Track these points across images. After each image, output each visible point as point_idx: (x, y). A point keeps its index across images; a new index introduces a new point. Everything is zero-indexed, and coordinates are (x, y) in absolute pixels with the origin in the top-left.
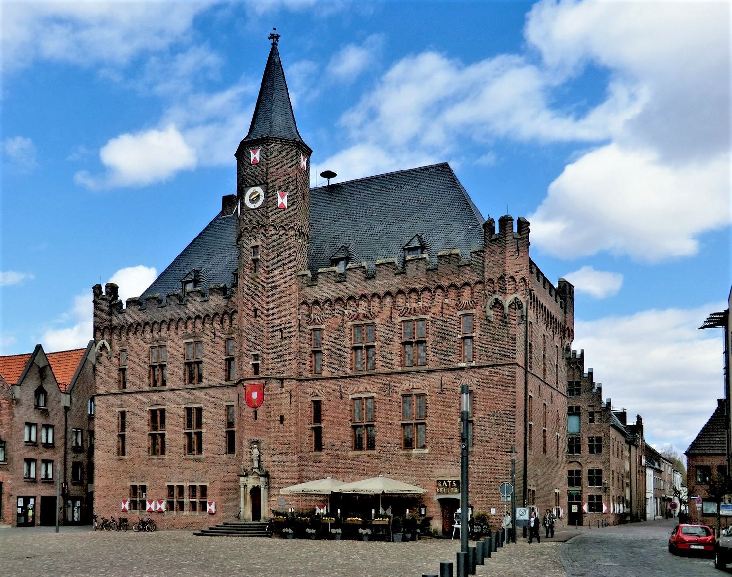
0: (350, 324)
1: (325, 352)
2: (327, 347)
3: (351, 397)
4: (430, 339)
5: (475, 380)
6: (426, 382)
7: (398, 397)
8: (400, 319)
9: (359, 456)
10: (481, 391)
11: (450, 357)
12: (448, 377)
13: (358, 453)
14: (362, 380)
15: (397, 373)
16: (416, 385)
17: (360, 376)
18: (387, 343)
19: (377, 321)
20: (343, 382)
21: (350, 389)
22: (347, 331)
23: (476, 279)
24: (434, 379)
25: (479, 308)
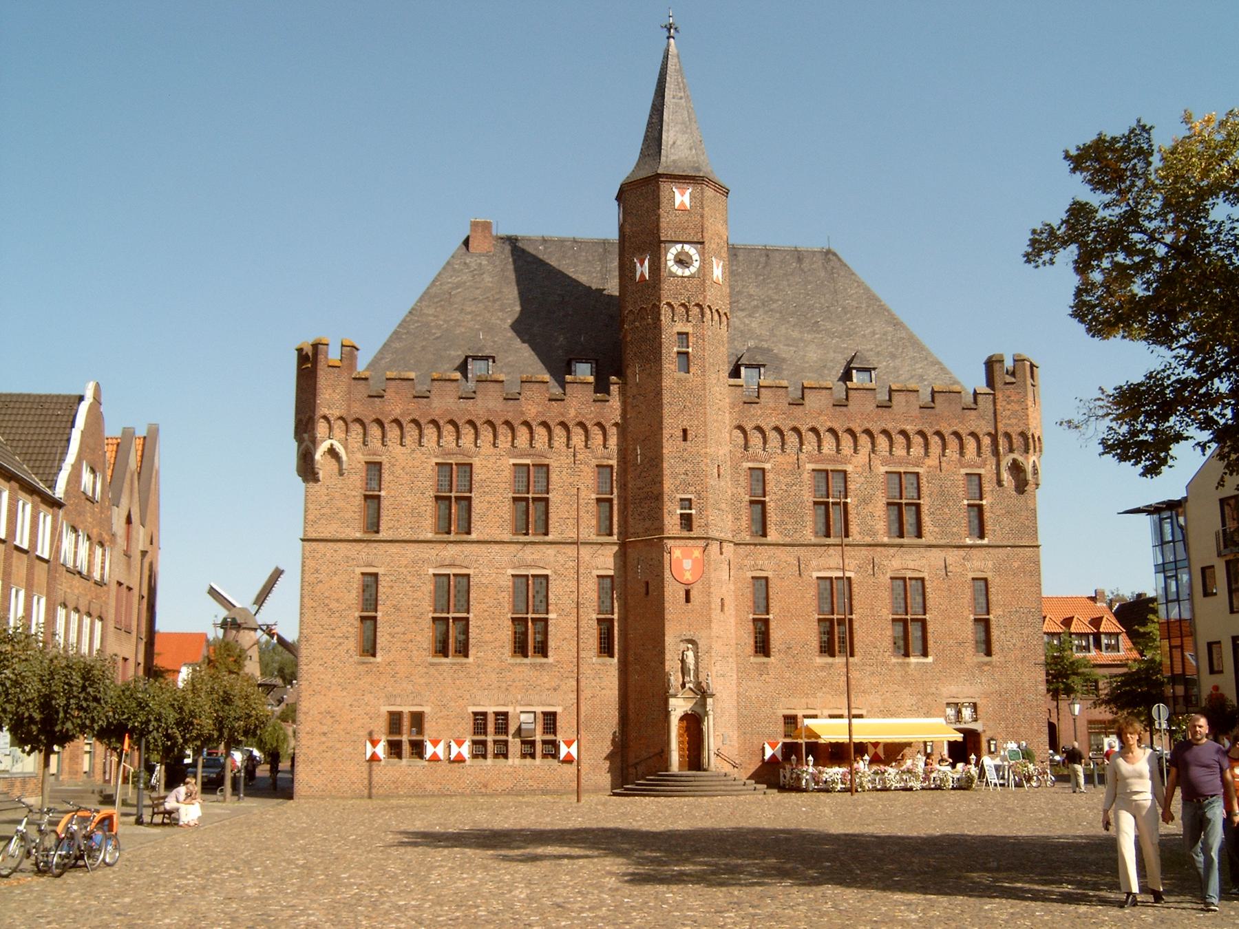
0: (810, 466)
1: (772, 504)
2: (774, 497)
3: (815, 574)
4: (925, 502)
5: (990, 564)
6: (924, 561)
7: (885, 579)
8: (883, 469)
9: (831, 665)
10: (998, 579)
11: (955, 530)
12: (953, 556)
13: (830, 660)
14: (831, 550)
15: (885, 545)
16: (911, 565)
17: (829, 545)
18: (865, 501)
19: (849, 468)
20: (801, 552)
21: (814, 563)
22: (806, 476)
23: (985, 430)
24: (936, 556)
25: (988, 467)
